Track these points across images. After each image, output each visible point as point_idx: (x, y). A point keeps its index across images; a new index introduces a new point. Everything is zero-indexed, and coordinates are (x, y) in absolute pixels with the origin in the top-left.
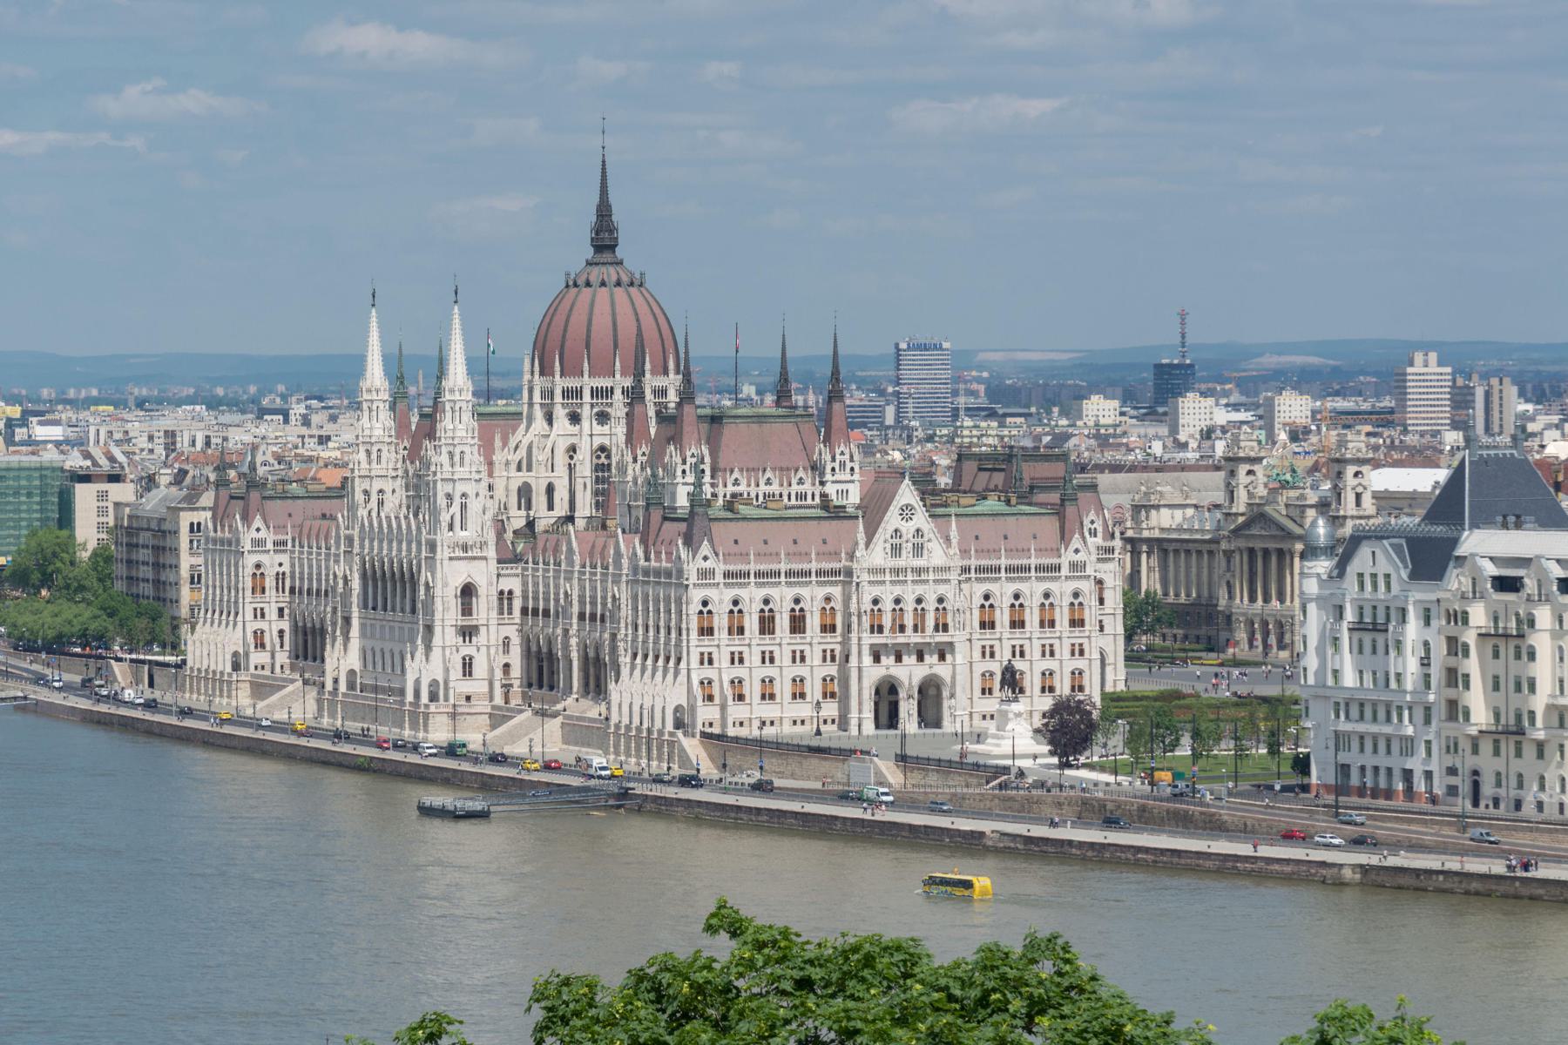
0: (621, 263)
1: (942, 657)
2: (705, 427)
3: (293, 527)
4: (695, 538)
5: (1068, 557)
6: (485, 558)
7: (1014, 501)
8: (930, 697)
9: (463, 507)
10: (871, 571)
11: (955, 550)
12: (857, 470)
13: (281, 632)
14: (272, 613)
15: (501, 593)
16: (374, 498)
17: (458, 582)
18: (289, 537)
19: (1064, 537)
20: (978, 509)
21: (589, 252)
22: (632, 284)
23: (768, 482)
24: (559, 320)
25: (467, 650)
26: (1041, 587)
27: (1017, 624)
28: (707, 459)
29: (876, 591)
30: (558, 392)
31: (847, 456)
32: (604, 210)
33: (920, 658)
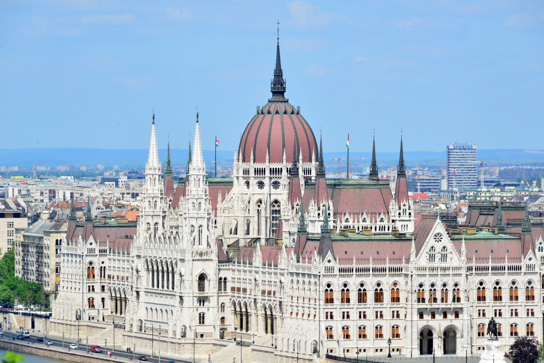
1: (457, 316)
2: (330, 190)
3: (110, 242)
4: (324, 250)
5: (524, 263)
6: (211, 260)
7: (496, 232)
8: (449, 336)
9: (200, 232)
10: (418, 269)
11: (464, 258)
12: (412, 214)
13: (103, 299)
14: (98, 288)
15: (221, 279)
17: (197, 273)
18: (107, 248)
19: (524, 252)
20: (477, 236)
22: (293, 113)
23: (364, 220)
27: (497, 298)
28: (332, 208)
29: (421, 280)
31: (407, 207)
32: (278, 74)
33: (445, 316)
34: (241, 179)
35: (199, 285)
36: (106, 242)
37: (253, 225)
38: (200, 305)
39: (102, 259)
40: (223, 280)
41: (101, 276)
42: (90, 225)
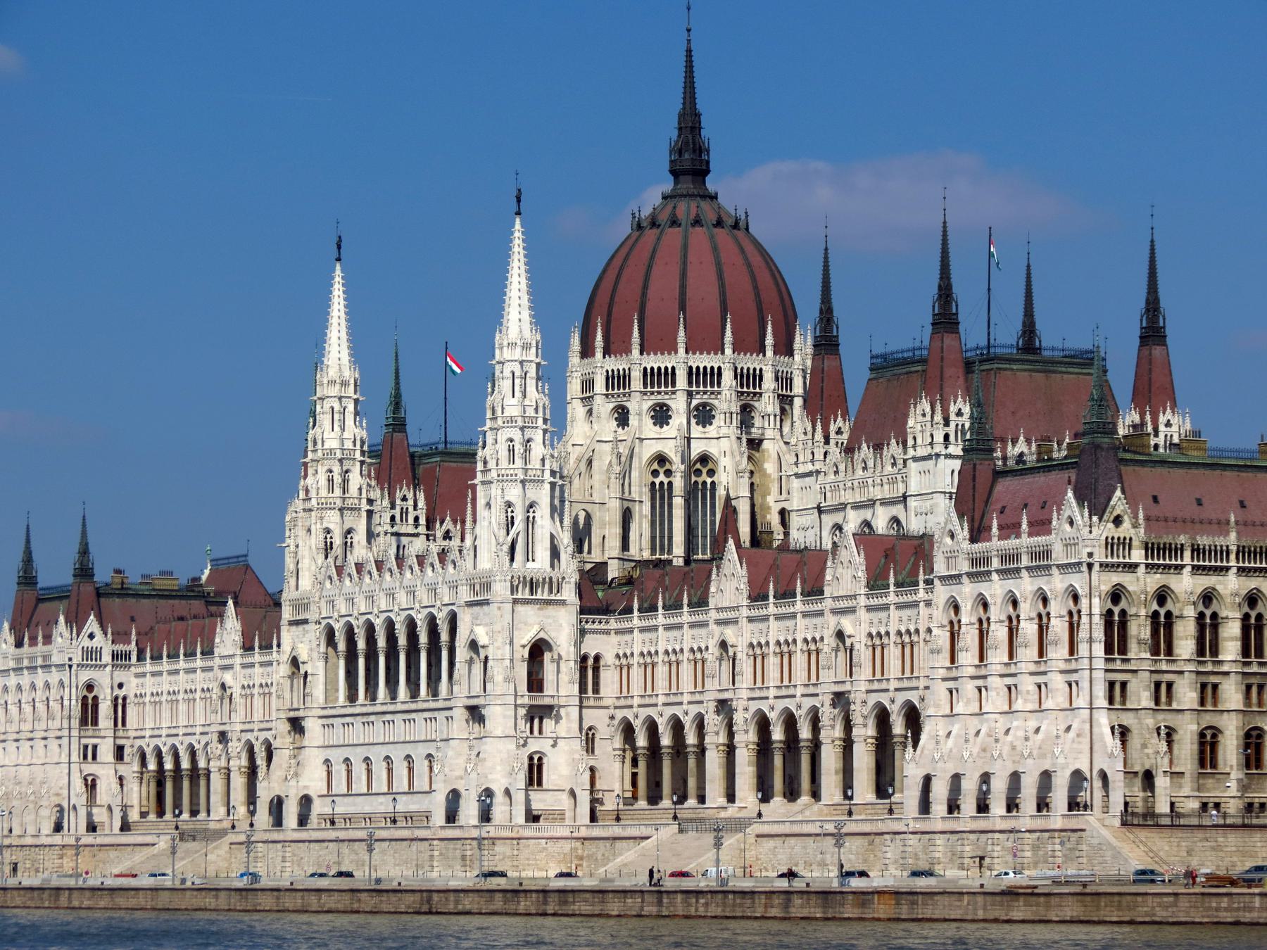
0: (714, 197)
3: (138, 634)
6: (562, 603)
15: (584, 658)
16: (338, 541)
17: (526, 637)
18: (133, 647)
21: (668, 185)
30: (636, 375)
32: (690, 122)
34: (599, 400)
35: (530, 674)
36: (128, 634)
37: (641, 527)
38: (532, 732)
39: (120, 676)
40: (590, 662)
41: (116, 724)
42: (88, 589)
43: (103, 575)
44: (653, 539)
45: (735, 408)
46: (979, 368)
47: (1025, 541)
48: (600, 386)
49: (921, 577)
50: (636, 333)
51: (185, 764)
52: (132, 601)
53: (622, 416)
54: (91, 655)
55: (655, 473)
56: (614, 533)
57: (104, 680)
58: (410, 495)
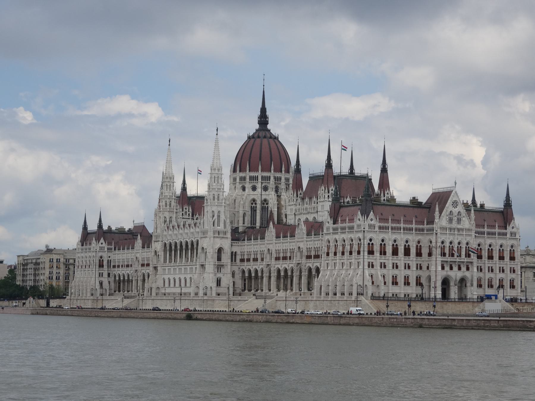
0: (269, 131)
6: (227, 238)
14: (105, 274)
15: (232, 253)
16: (168, 220)
17: (217, 246)
18: (113, 247)
21: (257, 126)
24: (248, 150)
25: (219, 275)
26: (500, 242)
29: (443, 238)
30: (248, 178)
32: (263, 110)
33: (460, 269)
34: (237, 184)
39: (110, 254)
43: (105, 228)
44: (251, 221)
45: (274, 187)
46: (339, 179)
47: (347, 225)
48: (238, 180)
49: (321, 233)
50: (248, 166)
51: (126, 278)
52: (113, 234)
53: (244, 189)
54: (102, 249)
55: (252, 204)
56: (241, 219)
57: (105, 256)
58: (187, 208)
